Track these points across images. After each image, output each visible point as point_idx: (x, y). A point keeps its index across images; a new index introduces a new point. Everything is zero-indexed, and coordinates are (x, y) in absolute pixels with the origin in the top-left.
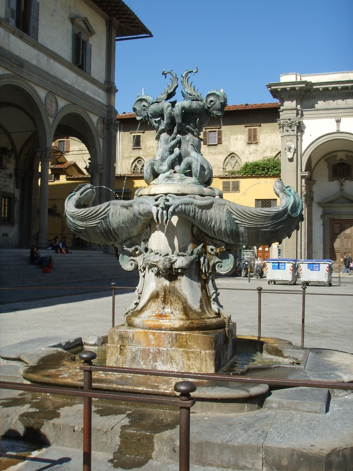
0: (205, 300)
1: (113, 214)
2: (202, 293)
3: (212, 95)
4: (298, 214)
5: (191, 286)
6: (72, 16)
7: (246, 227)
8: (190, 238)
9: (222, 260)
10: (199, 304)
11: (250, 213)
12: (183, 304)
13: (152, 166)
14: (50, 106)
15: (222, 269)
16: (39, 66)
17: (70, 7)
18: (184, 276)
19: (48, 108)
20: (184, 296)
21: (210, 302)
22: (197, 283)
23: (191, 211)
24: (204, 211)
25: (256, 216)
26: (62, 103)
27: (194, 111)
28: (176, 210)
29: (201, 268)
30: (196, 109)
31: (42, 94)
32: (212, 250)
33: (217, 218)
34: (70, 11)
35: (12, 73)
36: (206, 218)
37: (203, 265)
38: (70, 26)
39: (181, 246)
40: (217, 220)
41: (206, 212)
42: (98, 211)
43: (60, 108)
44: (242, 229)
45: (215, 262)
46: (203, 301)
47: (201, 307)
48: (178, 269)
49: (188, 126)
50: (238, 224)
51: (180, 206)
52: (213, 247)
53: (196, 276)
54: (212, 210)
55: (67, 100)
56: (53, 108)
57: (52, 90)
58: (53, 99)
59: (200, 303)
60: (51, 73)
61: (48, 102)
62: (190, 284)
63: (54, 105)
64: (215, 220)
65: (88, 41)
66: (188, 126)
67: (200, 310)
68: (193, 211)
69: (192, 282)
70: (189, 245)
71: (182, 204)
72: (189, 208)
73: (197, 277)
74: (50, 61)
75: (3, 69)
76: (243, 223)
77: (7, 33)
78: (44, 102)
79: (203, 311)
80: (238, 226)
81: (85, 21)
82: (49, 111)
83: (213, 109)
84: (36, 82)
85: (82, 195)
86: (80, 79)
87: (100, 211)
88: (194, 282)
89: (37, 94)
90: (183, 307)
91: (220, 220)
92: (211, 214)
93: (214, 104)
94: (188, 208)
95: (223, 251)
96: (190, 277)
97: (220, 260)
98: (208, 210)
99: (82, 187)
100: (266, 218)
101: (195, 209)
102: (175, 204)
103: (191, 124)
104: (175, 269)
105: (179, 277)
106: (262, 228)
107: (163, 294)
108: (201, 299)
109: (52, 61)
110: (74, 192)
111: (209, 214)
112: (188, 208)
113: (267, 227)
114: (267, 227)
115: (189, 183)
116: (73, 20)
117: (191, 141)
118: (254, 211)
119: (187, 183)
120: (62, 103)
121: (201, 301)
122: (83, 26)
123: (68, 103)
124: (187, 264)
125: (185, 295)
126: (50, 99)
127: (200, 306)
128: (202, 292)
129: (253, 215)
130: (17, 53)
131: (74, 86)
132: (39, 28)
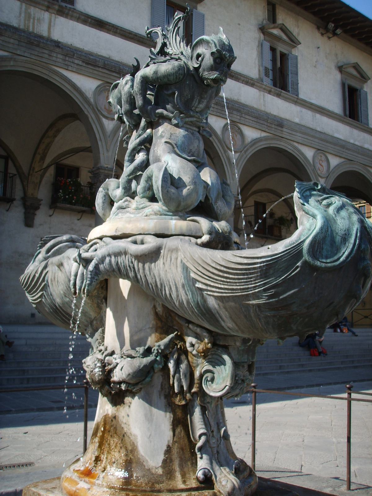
0: (182, 449)
1: (51, 279)
2: (174, 435)
3: (199, 45)
4: (341, 259)
5: (149, 419)
6: (340, 64)
7: (218, 297)
8: (151, 321)
9: (214, 367)
10: (161, 457)
11: (214, 265)
12: (126, 455)
13: (106, 191)
14: (319, 166)
15: (214, 386)
16: (303, 123)
17: (336, 55)
18: (136, 398)
19: (317, 168)
20: (132, 438)
21: (194, 455)
22: (162, 413)
23: (128, 268)
24: (147, 266)
25: (225, 269)
26: (334, 161)
27: (166, 80)
28: (101, 267)
29: (171, 382)
30: (167, 76)
31: (309, 153)
32: (192, 345)
33: (170, 280)
34: (337, 59)
35: (272, 135)
36: (154, 280)
37: (174, 377)
38: (338, 76)
39: (136, 338)
40: (171, 284)
41: (150, 269)
42: (34, 276)
43: (332, 167)
44: (212, 302)
45: (203, 371)
46: (175, 450)
47: (167, 463)
48: (120, 383)
49: (159, 111)
50: (201, 290)
51: (107, 259)
52: (194, 340)
53: (163, 397)
54: (160, 262)
55: (340, 157)
56: (324, 167)
57: (319, 148)
58: (323, 158)
59: (165, 454)
60: (319, 129)
61: (317, 161)
62: (146, 415)
63: (324, 164)
64: (168, 283)
65: (362, 88)
66: (159, 111)
67: (160, 471)
68: (129, 266)
69: (151, 411)
70: (150, 335)
71: (109, 255)
72: (123, 262)
73: (163, 401)
74: (315, 117)
75: (260, 132)
76: (209, 288)
77: (262, 93)
78: (312, 163)
79: (169, 473)
80: (203, 294)
81: (356, 67)
82: (319, 172)
83: (204, 70)
84: (300, 142)
85: (50, 253)
86: (356, 132)
87: (37, 275)
88: (155, 410)
89: (302, 154)
90: (126, 461)
91: (175, 283)
92: (159, 271)
93: (203, 59)
94: (122, 261)
95: (207, 349)
96: (148, 400)
97: (211, 368)
98: (153, 264)
99: (50, 240)
100: (247, 274)
101: (132, 262)
102: (98, 256)
103: (169, 106)
104: (114, 382)
105: (128, 399)
106: (247, 297)
107: (102, 429)
108: (168, 446)
109: (318, 116)
110: (39, 249)
111: (156, 272)
112: (122, 261)
113: (256, 296)
114: (256, 296)
115: (148, 214)
116: (340, 69)
117: (167, 135)
118: (221, 259)
119: (145, 214)
120: (334, 161)
121: (168, 451)
122: (354, 73)
123: (342, 160)
124: (129, 374)
125: (134, 435)
126: (320, 158)
127: (165, 462)
128: (174, 431)
129: (222, 269)
130: (275, 112)
131: (348, 140)
132: (299, 82)
